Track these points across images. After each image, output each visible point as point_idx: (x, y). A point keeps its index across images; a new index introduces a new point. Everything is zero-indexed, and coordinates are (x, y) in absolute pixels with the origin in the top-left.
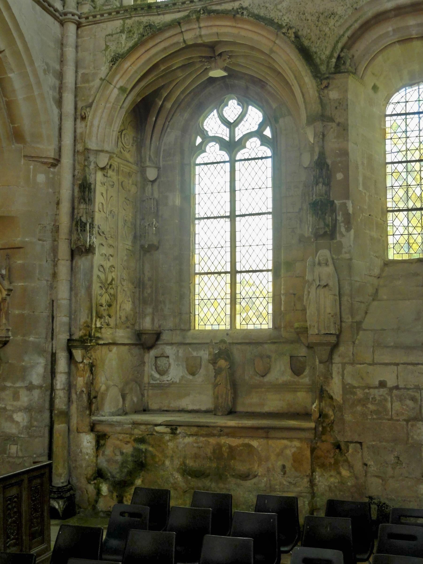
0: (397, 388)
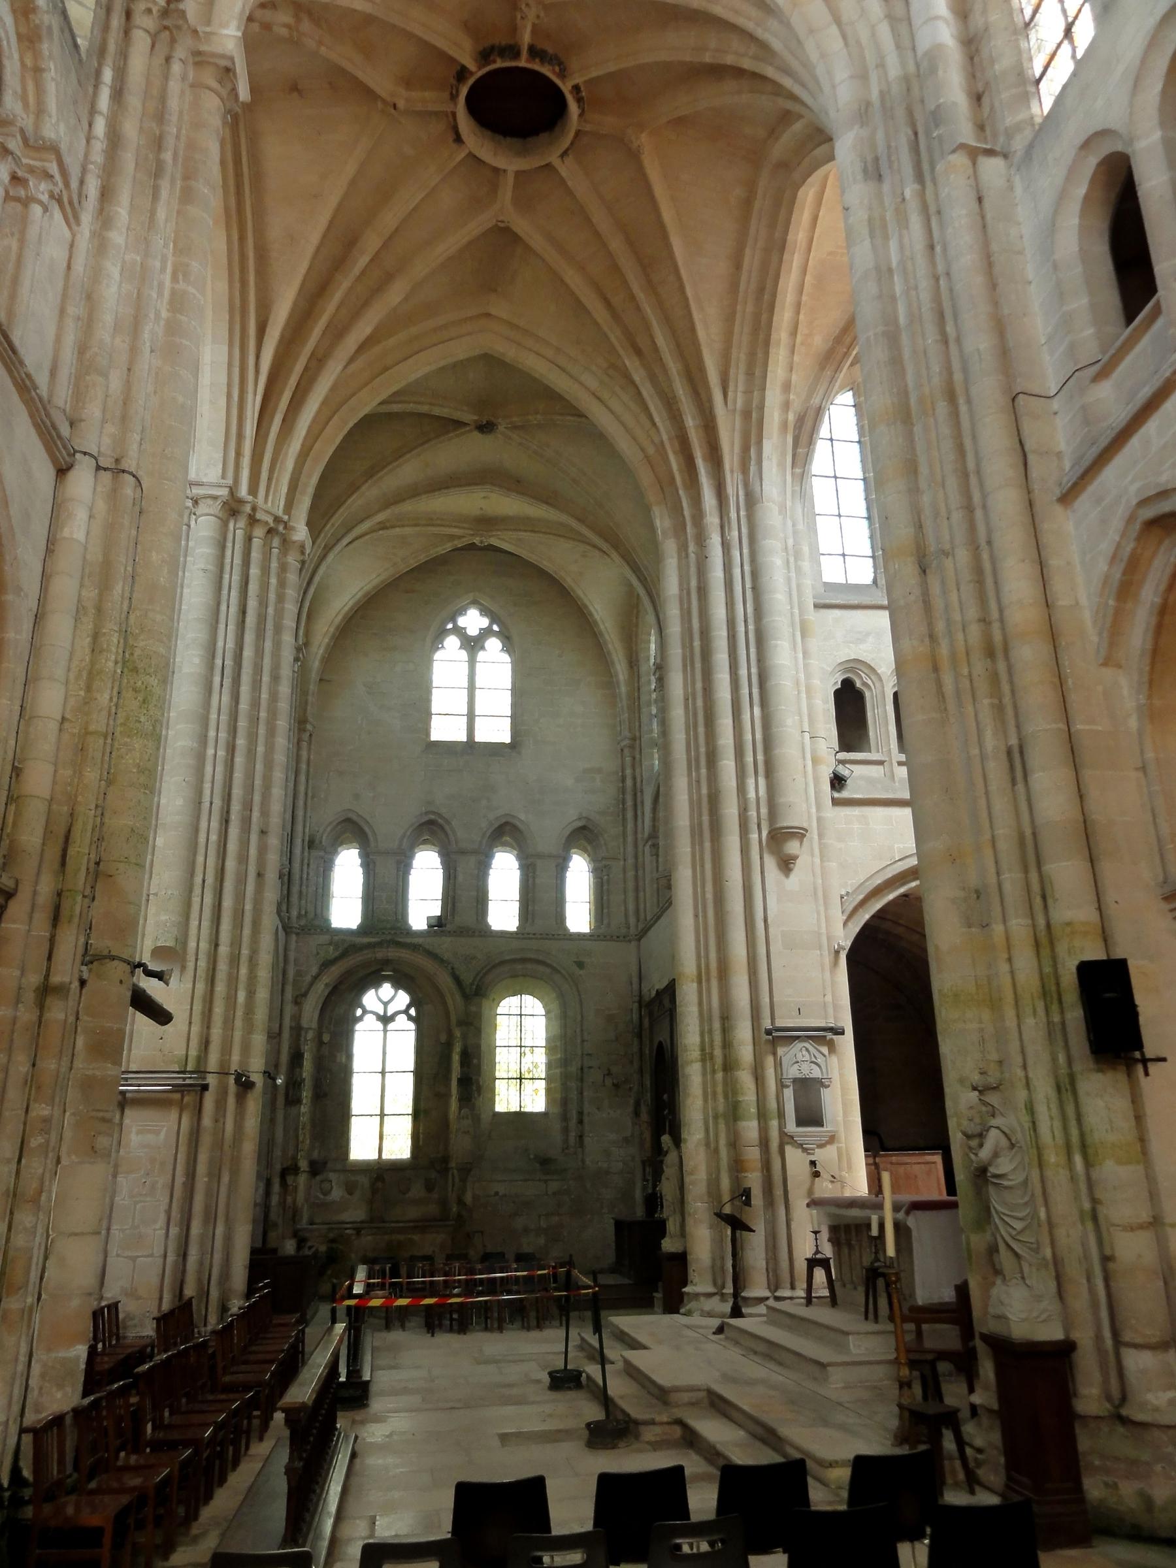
0: (505, 1195)
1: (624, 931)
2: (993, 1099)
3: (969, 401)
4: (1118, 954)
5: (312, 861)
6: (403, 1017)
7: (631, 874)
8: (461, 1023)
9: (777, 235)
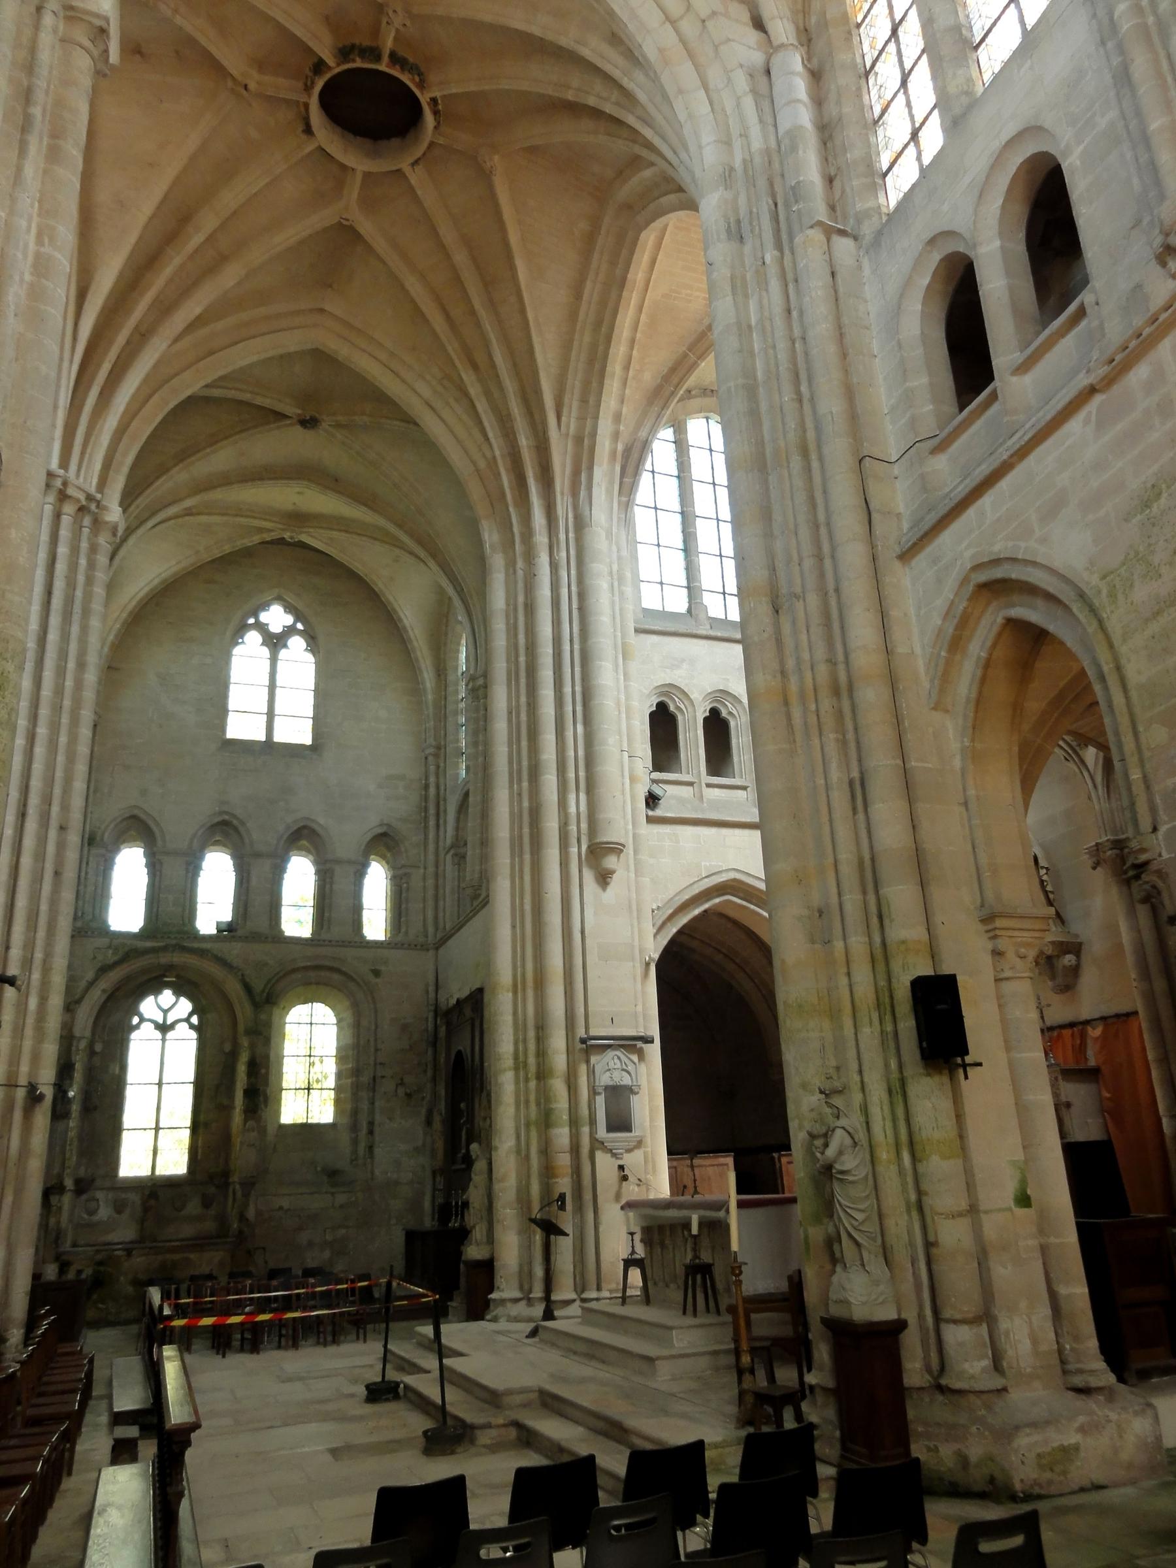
0: (289, 1210)
1: (421, 939)
2: (837, 1101)
3: (821, 459)
4: (946, 970)
5: (91, 859)
6: (185, 1025)
7: (430, 882)
8: (248, 1032)
9: (618, 272)
